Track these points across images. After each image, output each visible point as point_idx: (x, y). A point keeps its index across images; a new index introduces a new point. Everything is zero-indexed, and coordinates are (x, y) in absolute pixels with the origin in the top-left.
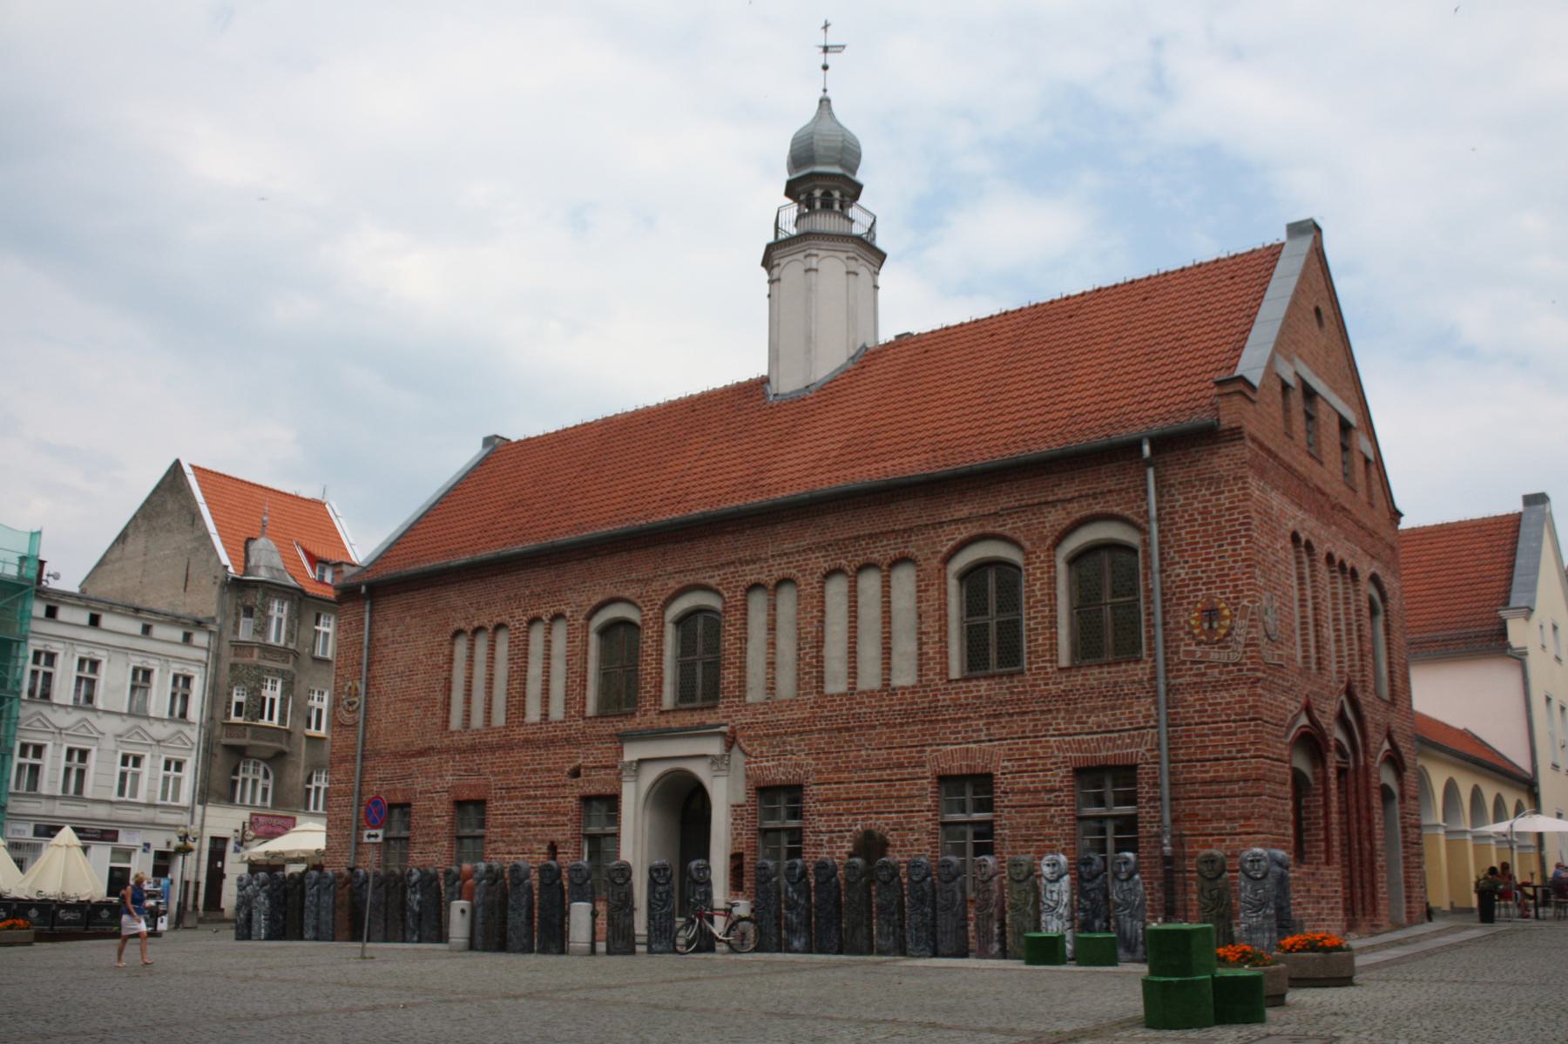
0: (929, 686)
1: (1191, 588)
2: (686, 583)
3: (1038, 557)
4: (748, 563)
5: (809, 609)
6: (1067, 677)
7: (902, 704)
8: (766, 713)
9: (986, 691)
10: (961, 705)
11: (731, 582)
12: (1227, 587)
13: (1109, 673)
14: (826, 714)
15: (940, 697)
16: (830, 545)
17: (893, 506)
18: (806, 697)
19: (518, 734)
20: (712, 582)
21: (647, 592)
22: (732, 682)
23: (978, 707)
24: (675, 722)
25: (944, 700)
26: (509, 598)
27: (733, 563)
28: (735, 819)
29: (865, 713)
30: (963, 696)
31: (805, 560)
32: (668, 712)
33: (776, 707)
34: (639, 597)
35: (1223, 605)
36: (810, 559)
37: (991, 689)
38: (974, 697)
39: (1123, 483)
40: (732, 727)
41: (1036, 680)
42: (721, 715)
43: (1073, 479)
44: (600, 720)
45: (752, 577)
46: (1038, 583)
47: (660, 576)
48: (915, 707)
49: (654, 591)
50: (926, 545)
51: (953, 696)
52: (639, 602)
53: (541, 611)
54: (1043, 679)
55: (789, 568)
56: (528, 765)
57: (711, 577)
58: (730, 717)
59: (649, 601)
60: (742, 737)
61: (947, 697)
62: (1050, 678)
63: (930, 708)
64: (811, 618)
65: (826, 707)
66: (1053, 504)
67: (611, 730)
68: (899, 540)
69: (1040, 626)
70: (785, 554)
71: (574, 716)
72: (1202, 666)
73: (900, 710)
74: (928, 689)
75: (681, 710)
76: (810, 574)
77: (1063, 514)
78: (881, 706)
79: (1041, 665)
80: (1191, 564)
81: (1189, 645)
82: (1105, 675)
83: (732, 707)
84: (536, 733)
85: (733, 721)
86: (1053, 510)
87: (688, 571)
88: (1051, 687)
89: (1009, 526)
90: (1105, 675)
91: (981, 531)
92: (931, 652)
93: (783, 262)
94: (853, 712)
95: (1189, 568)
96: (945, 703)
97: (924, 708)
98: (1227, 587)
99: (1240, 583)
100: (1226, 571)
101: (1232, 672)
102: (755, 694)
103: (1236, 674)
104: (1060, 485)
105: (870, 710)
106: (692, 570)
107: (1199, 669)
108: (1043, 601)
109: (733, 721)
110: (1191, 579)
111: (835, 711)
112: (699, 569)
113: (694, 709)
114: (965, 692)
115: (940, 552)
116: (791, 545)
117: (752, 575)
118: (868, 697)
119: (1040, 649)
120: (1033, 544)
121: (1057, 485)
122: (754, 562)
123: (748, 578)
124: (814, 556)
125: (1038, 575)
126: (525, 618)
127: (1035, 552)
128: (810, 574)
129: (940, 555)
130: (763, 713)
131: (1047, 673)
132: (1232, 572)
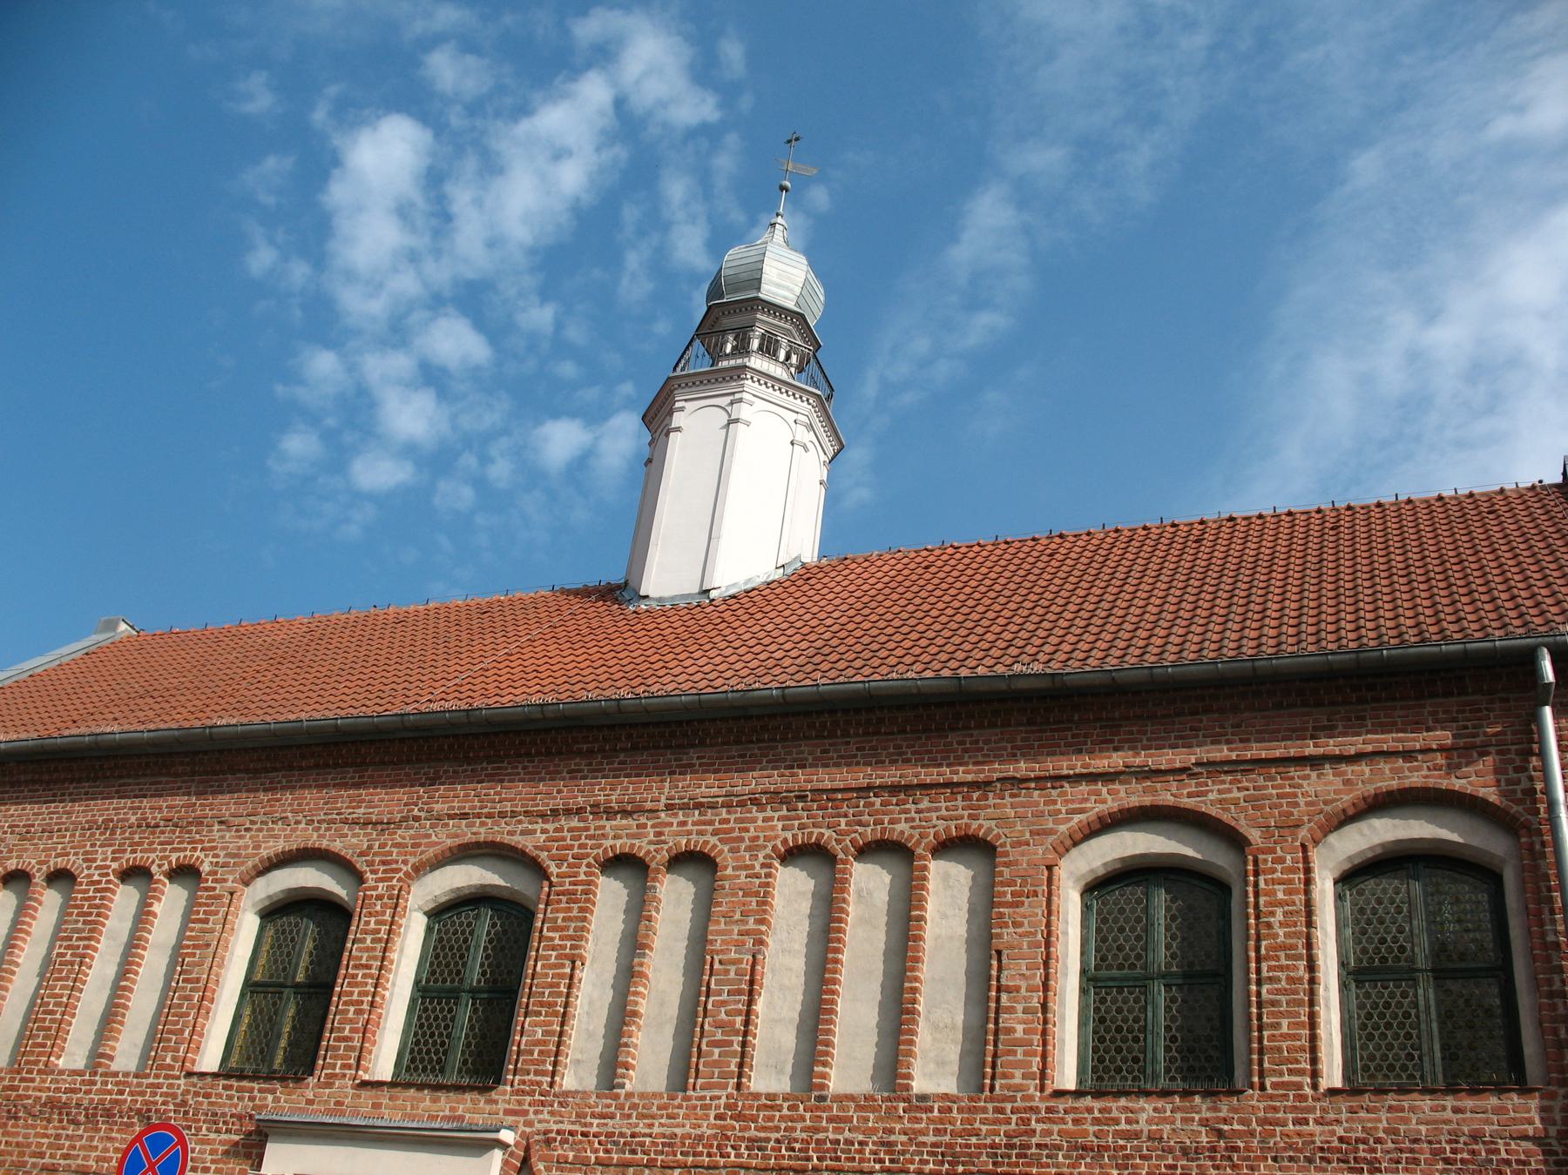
0: (1013, 1099)
2: (468, 838)
3: (1282, 860)
4: (610, 813)
5: (737, 916)
6: (1352, 1111)
7: (937, 1132)
8: (612, 1117)
9: (1149, 1121)
10: (1084, 1148)
11: (571, 847)
13: (1456, 1110)
14: (753, 1133)
15: (1039, 1127)
16: (802, 798)
17: (952, 737)
18: (708, 1094)
19: (38, 1089)
20: (527, 843)
21: (382, 846)
22: (538, 1043)
23: (1127, 1157)
24: (395, 1111)
25: (1048, 1133)
26: (92, 825)
27: (580, 811)
29: (849, 1142)
30: (1092, 1129)
31: (741, 820)
32: (379, 1084)
33: (634, 1106)
34: (361, 854)
36: (754, 820)
37: (1165, 1120)
38: (1117, 1134)
39: (1474, 736)
40: (523, 1134)
41: (1275, 1109)
42: (502, 1106)
43: (1363, 718)
44: (222, 1082)
45: (618, 843)
46: (1279, 912)
47: (416, 819)
48: (974, 1140)
49: (396, 845)
50: (1022, 817)
51: (1070, 1126)
52: (361, 865)
53: (153, 856)
54: (1294, 1109)
55: (700, 833)
56: (42, 1155)
57: (524, 833)
58: (526, 1113)
59: (384, 863)
61: (1056, 1128)
62: (1311, 1110)
63: (1010, 1146)
64: (741, 933)
65: (754, 1119)
66: (1315, 762)
67: (242, 1107)
68: (960, 803)
69: (1283, 998)
70: (698, 806)
71: (171, 1067)
73: (934, 1145)
74: (1009, 1106)
75: (408, 1085)
76: (748, 849)
77: (1338, 783)
78: (891, 1131)
79: (1286, 1078)
82: (1449, 1114)
83: (532, 1093)
84: (73, 1091)
85: (529, 1124)
86: (1314, 775)
87: (479, 816)
88: (1312, 1127)
89: (1211, 796)
90: (1449, 1114)
91: (1147, 800)
92: (1020, 1028)
93: (690, 406)
94: (821, 1136)
96: (1047, 1140)
97: (993, 1146)
102: (579, 1073)
104: (1333, 728)
105: (861, 1137)
106: (490, 816)
108: (1292, 947)
111: (777, 1129)
112: (502, 815)
113: (438, 1087)
114: (1096, 1121)
115: (1051, 832)
116: (715, 791)
117: (615, 837)
118: (859, 1108)
119: (1284, 1045)
120: (1267, 835)
121: (1324, 728)
122: (626, 813)
123: (608, 843)
124: (761, 816)
125: (1280, 895)
126: (115, 865)
127: (1273, 851)
128: (748, 849)
129: (1051, 839)
130: (602, 1116)
131: (1303, 1098)
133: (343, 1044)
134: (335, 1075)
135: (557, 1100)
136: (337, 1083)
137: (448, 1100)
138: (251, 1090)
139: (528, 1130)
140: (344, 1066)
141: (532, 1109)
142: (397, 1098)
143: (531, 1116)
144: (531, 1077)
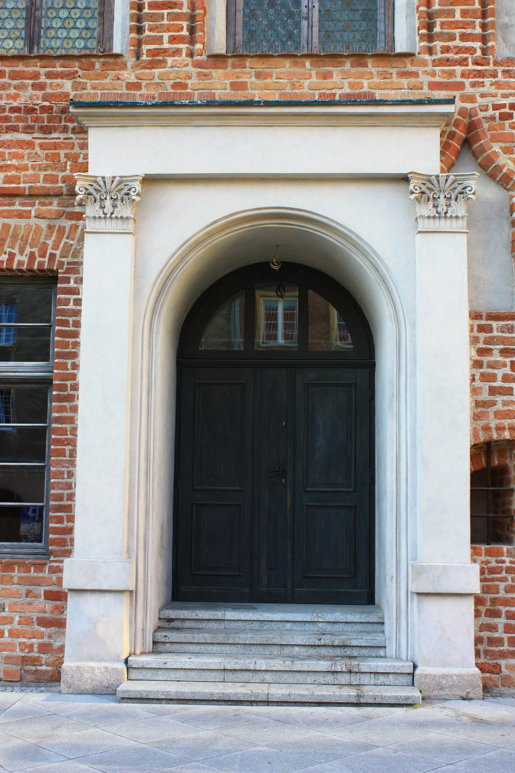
28: (481, 352)
42: (425, 79)
58: (460, 86)
60: (495, 139)
83: (463, 62)
85: (471, 99)
109: (466, 98)
133: (165, 12)
134: (165, 51)
135: (500, 69)
136: (170, 60)
137: (346, 75)
138: (36, 76)
139: (469, 106)
140: (173, 40)
141: (467, 82)
142: (269, 75)
143: (469, 90)
144: (458, 42)
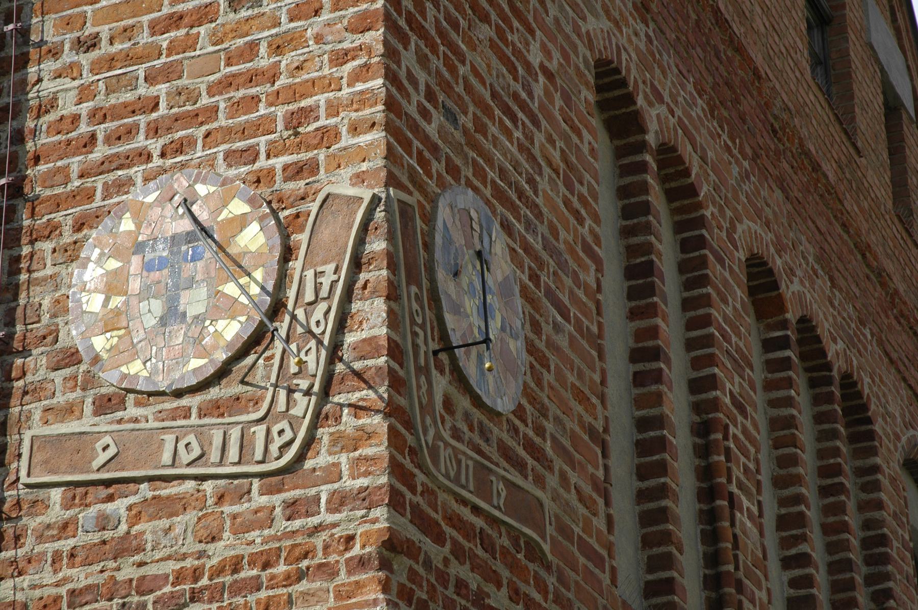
1: (100, 152)
12: (263, 126)
35: (238, 207)
72: (120, 506)
80: (105, 49)
81: (70, 411)
95: (96, 68)
98: (263, 126)
99: (322, 99)
100: (264, 61)
101: (265, 518)
103: (281, 525)
107: (103, 522)
110: (99, 116)
132: (288, 60)
